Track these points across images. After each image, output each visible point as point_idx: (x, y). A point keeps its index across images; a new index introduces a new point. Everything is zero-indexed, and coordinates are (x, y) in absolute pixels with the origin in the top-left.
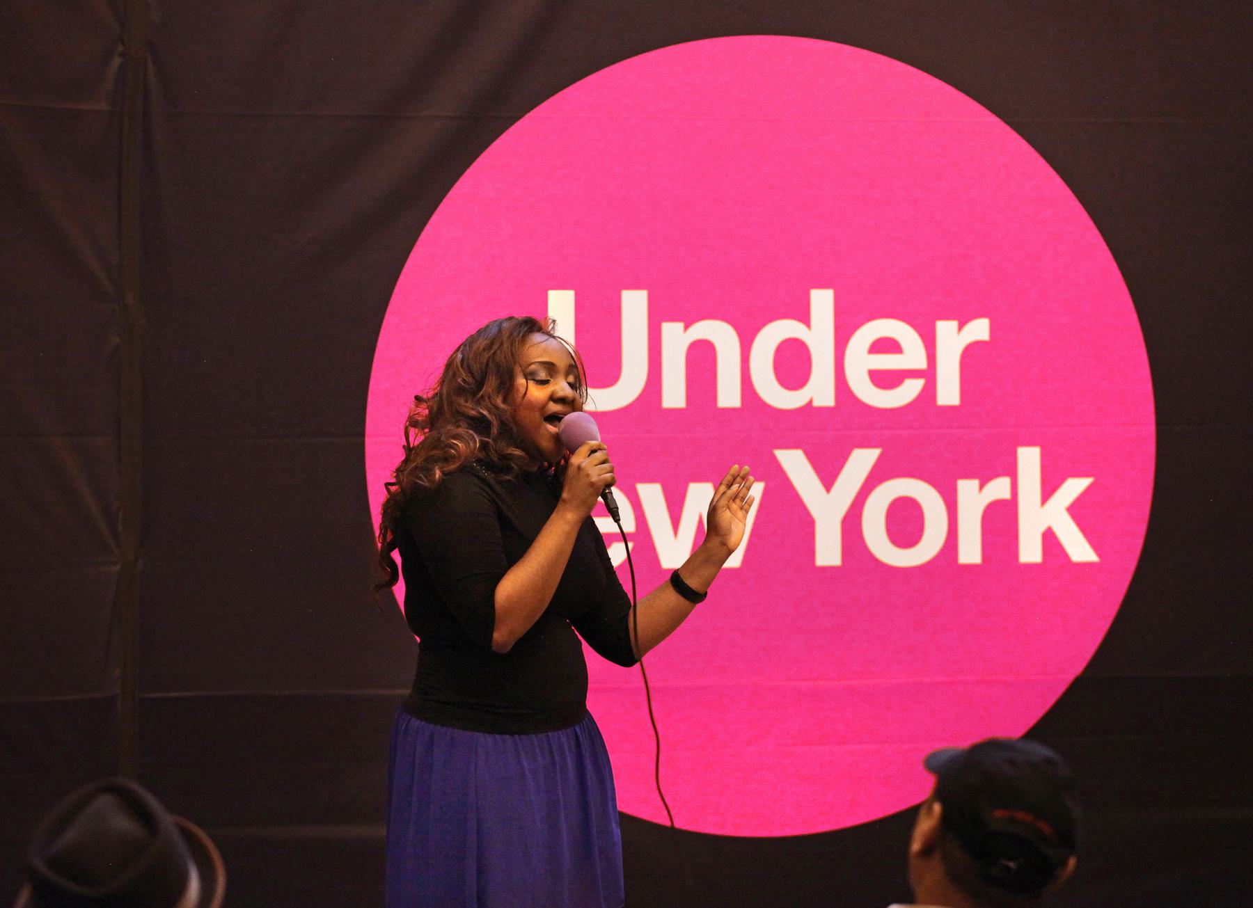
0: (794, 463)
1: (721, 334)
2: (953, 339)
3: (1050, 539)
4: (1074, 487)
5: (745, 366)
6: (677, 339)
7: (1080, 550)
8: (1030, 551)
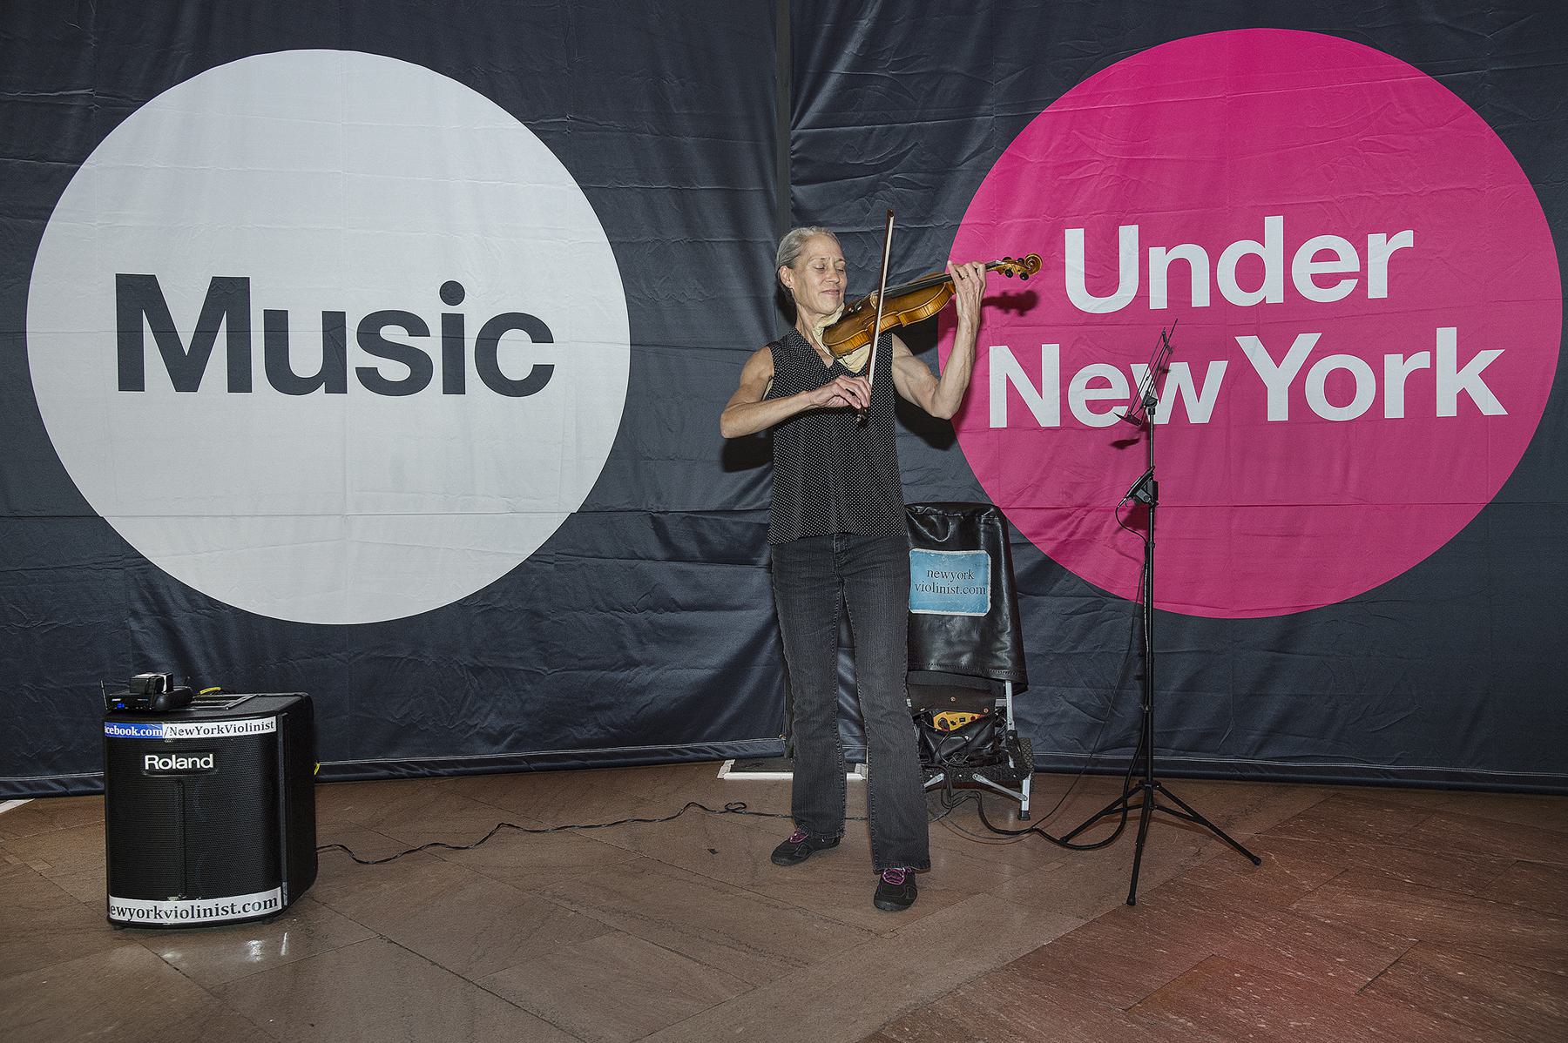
0: (1251, 346)
1: (1195, 254)
2: (1381, 248)
3: (1464, 398)
4: (1486, 358)
5: (1213, 276)
6: (1160, 259)
7: (1489, 405)
8: (1446, 407)
